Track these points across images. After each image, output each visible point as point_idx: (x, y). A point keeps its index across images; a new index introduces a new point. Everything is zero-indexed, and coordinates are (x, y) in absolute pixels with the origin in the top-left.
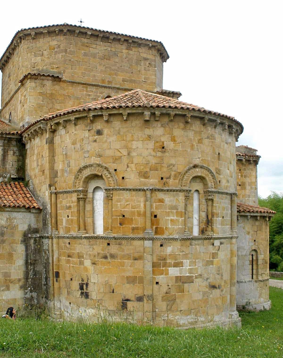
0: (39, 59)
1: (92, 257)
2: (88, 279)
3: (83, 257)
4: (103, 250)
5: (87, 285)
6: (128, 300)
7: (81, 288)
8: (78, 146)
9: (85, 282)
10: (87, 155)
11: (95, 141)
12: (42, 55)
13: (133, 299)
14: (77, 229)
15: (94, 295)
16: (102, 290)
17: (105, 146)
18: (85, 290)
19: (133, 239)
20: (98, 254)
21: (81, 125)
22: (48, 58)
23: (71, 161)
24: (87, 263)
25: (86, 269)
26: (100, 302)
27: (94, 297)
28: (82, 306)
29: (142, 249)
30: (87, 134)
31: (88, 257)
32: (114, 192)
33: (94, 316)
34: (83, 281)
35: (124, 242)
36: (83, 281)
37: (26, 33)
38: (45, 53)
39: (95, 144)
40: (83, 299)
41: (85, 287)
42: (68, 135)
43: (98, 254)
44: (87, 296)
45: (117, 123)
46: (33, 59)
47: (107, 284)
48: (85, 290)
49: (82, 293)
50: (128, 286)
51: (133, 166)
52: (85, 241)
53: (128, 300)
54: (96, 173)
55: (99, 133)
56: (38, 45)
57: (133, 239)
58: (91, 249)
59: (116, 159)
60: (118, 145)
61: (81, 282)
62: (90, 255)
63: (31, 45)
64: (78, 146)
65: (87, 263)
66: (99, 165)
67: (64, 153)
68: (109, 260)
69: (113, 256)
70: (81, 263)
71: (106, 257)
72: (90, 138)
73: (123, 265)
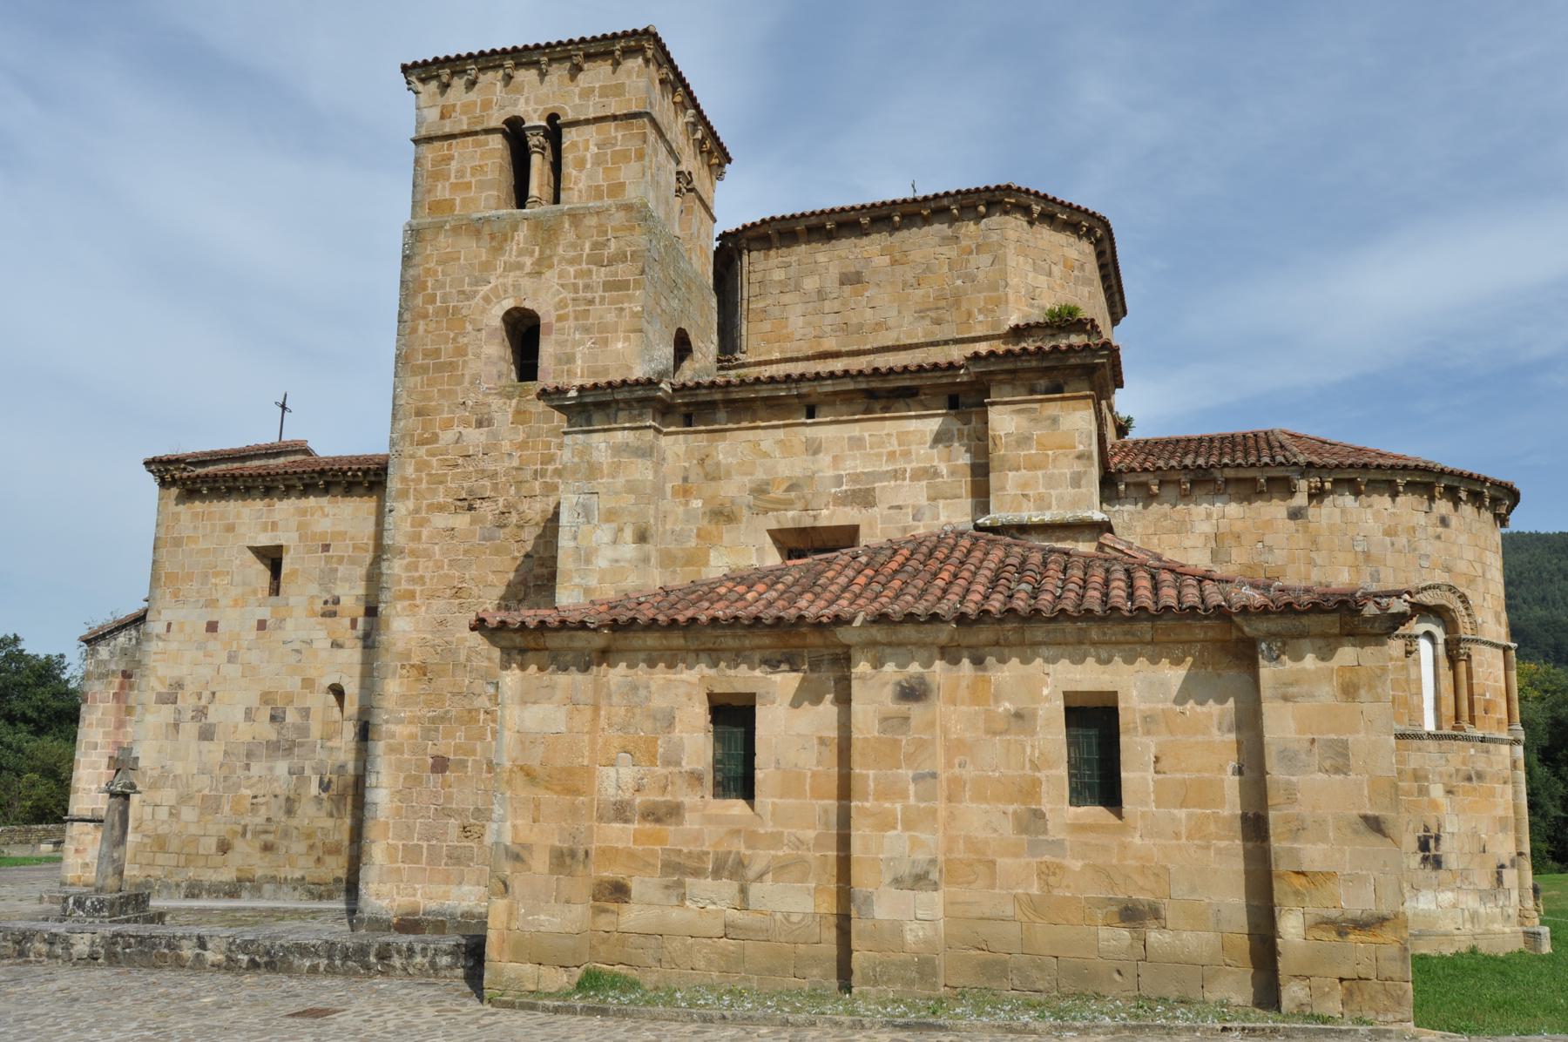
0: (1042, 280)
1: (1446, 779)
2: (1439, 827)
3: (1426, 778)
4: (1464, 763)
5: (1437, 838)
6: (1502, 866)
7: (1424, 845)
8: (1402, 540)
9: (1433, 832)
10: (1425, 563)
11: (1439, 537)
12: (1050, 274)
13: (1508, 863)
14: (1406, 719)
15: (1452, 861)
16: (1467, 849)
17: (1455, 549)
18: (1433, 852)
19: (1502, 741)
20: (1458, 771)
21: (1406, 501)
22: (1063, 287)
23: (1382, 568)
24: (1437, 791)
25: (1434, 805)
26: (1464, 874)
27: (1454, 866)
28: (1428, 887)
29: (1508, 762)
30: (1421, 519)
31: (1437, 778)
32: (1473, 646)
33: (1455, 906)
34: (1427, 829)
35: (1492, 746)
36: (1427, 829)
37: (1024, 199)
38: (1056, 270)
39: (1437, 543)
40: (1428, 870)
41: (1432, 843)
42: (1369, 511)
43: (1458, 771)
44: (1437, 863)
45: (1467, 510)
46: (1031, 275)
47: (1475, 834)
48: (1433, 852)
49: (1425, 859)
50: (1500, 835)
51: (1488, 597)
52: (1432, 745)
53: (1502, 866)
54: (1444, 602)
55: (1444, 521)
56: (1040, 244)
57: (1502, 741)
58: (1443, 762)
59: (1472, 581)
60: (1469, 554)
61: (1421, 833)
62: (1441, 775)
63: (1025, 236)
64: (1402, 540)
65: (1437, 791)
66: (1451, 589)
67: (1359, 549)
68: (1475, 783)
69: (1480, 776)
70: (1423, 791)
71: (1469, 779)
72: (1430, 529)
73: (1492, 793)
